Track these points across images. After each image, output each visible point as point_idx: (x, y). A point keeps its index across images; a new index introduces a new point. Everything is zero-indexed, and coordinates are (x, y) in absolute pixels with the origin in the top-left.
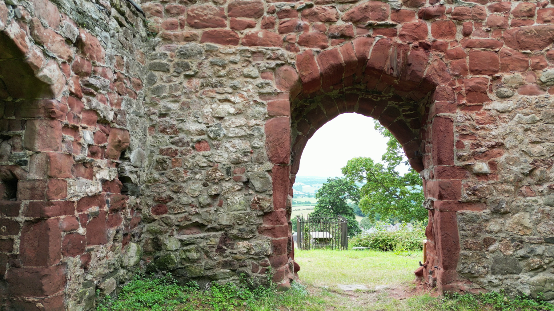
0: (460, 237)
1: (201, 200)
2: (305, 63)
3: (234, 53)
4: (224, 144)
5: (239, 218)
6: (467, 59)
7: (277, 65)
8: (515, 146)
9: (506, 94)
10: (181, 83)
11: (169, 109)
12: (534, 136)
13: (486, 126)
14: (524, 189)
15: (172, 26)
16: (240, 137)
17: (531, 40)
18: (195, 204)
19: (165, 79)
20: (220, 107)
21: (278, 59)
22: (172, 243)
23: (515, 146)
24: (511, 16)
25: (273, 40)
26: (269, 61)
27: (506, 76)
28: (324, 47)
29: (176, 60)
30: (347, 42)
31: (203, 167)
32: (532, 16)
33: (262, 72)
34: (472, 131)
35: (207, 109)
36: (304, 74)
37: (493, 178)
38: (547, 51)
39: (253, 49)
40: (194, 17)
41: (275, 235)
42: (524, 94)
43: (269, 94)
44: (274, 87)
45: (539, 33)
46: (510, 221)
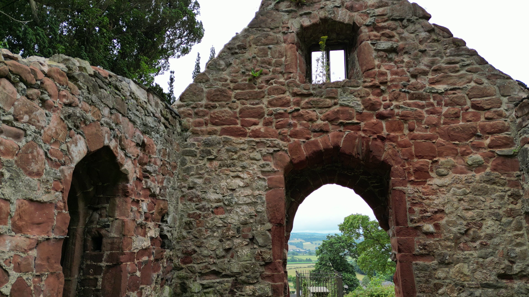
0: (416, 282)
1: (218, 252)
2: (295, 149)
3: (243, 143)
4: (235, 209)
5: (246, 267)
6: (413, 148)
7: (274, 151)
8: (453, 212)
9: (443, 173)
10: (205, 165)
11: (195, 184)
12: (466, 205)
13: (430, 197)
14: (461, 245)
15: (200, 124)
16: (247, 204)
17: (458, 135)
18: (213, 255)
19: (193, 161)
20: (233, 181)
21: (275, 147)
23: (453, 212)
24: (443, 117)
25: (271, 133)
26: (269, 149)
27: (442, 160)
28: (308, 139)
29: (202, 148)
30: (325, 135)
31: (219, 227)
32: (458, 117)
33: (264, 156)
34: (420, 200)
35: (223, 183)
36: (294, 157)
37: (437, 237)
38: (471, 142)
39: (257, 140)
40: (215, 118)
41: (274, 281)
42: (456, 173)
43: (269, 172)
44: (272, 166)
45: (464, 129)
46: (453, 270)
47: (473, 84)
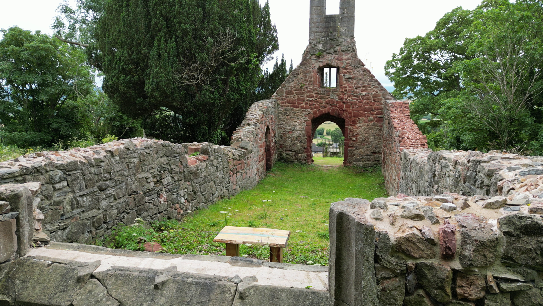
2: (315, 113)
15: (283, 103)
22: (284, 154)
35: (292, 124)
45: (369, 108)
47: (375, 92)
